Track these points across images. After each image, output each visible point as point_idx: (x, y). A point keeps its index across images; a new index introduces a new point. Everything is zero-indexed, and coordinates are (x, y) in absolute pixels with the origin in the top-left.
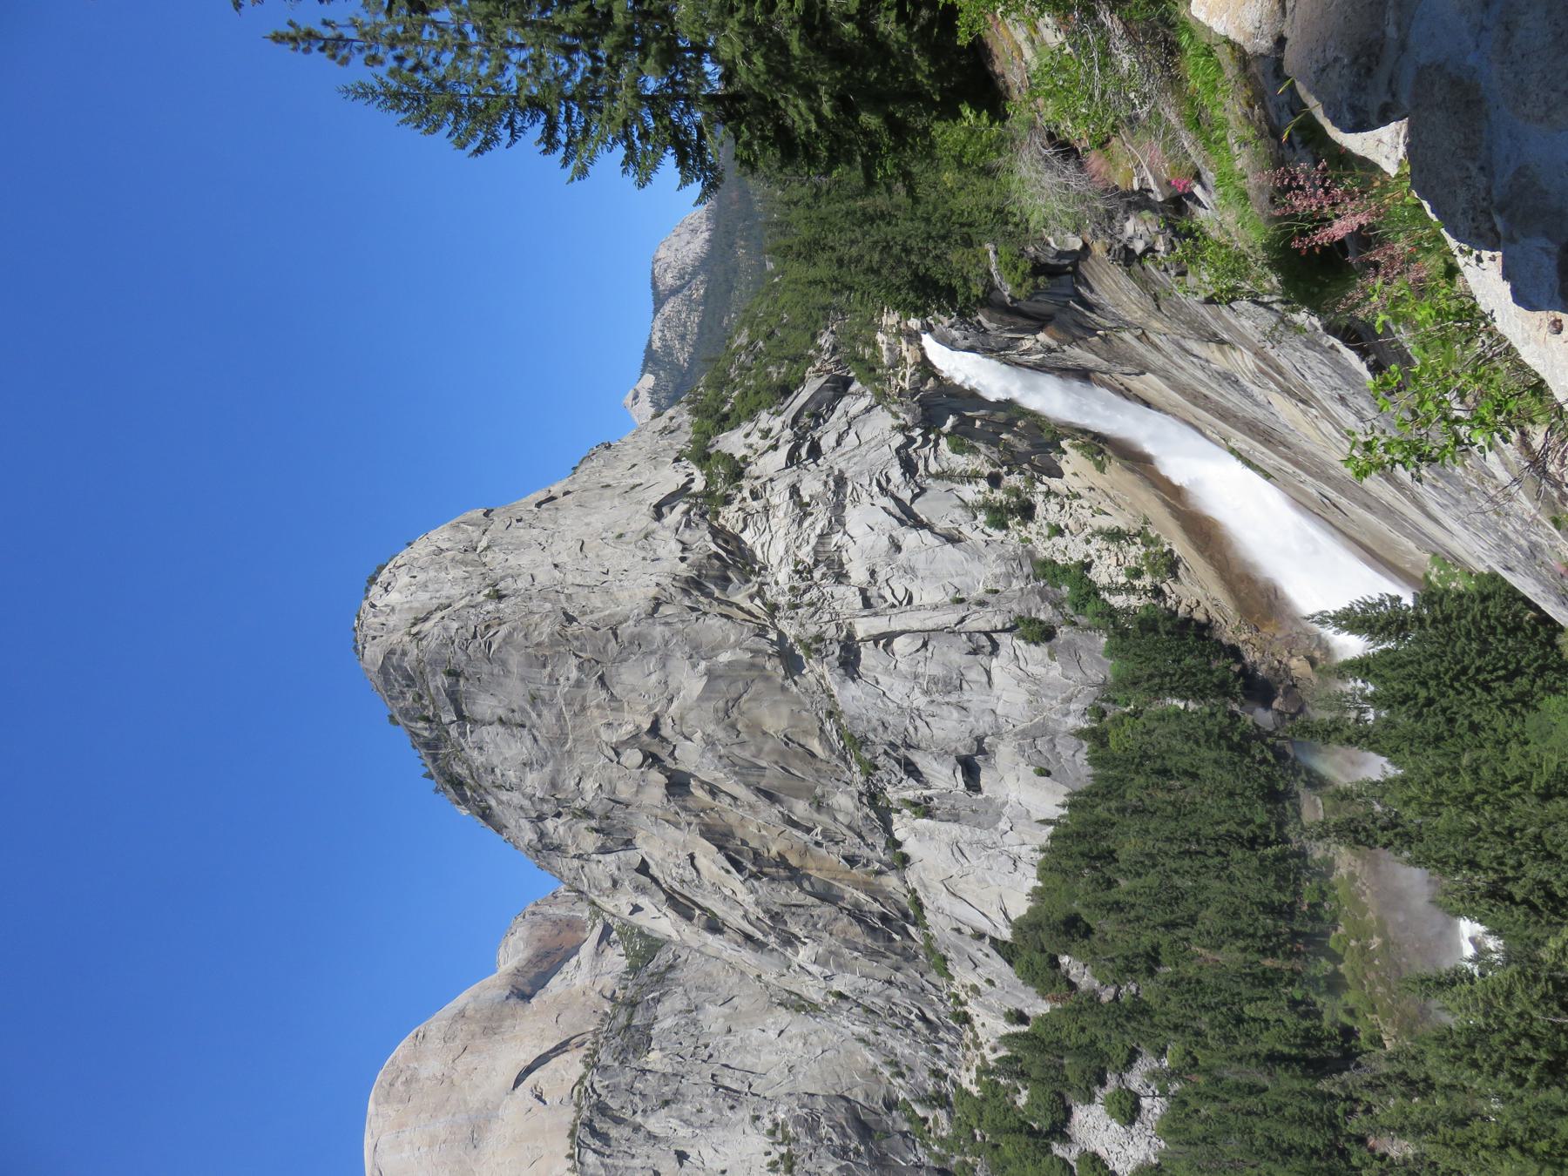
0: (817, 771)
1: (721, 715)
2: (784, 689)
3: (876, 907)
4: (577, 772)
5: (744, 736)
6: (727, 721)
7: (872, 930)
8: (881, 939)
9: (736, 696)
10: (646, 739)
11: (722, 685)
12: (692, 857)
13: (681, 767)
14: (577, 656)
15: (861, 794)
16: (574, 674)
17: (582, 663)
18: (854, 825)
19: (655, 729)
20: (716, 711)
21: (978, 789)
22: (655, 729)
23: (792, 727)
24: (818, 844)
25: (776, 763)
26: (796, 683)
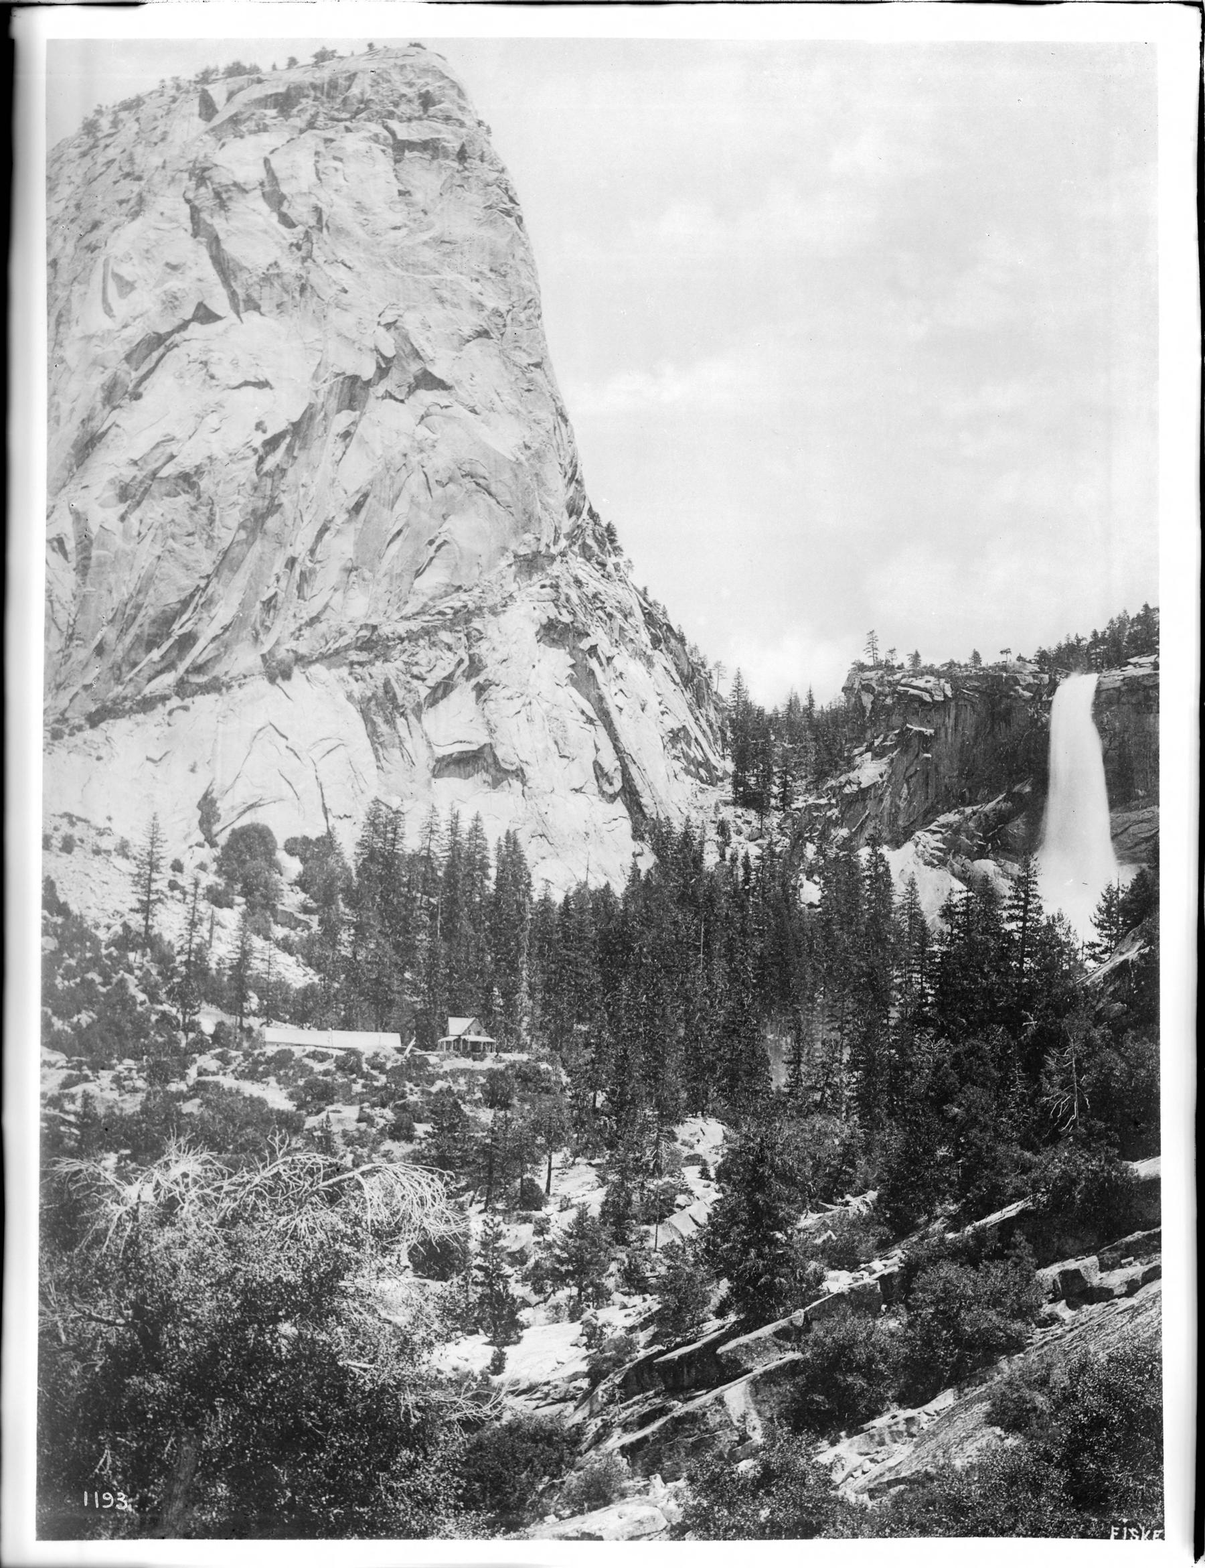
0: (400, 576)
1: (467, 468)
2: (504, 549)
3: (208, 631)
4: (358, 267)
5: (438, 491)
6: (458, 473)
7: (166, 620)
8: (153, 630)
9: (493, 489)
10: (415, 367)
11: (507, 476)
12: (263, 384)
13: (372, 402)
14: (508, 311)
15: (375, 628)
16: (490, 304)
17: (501, 316)
18: (329, 611)
19: (427, 381)
20: (471, 462)
21: (437, 773)
22: (427, 381)
23: (460, 551)
24: (291, 562)
25: (407, 525)
26: (510, 565)
